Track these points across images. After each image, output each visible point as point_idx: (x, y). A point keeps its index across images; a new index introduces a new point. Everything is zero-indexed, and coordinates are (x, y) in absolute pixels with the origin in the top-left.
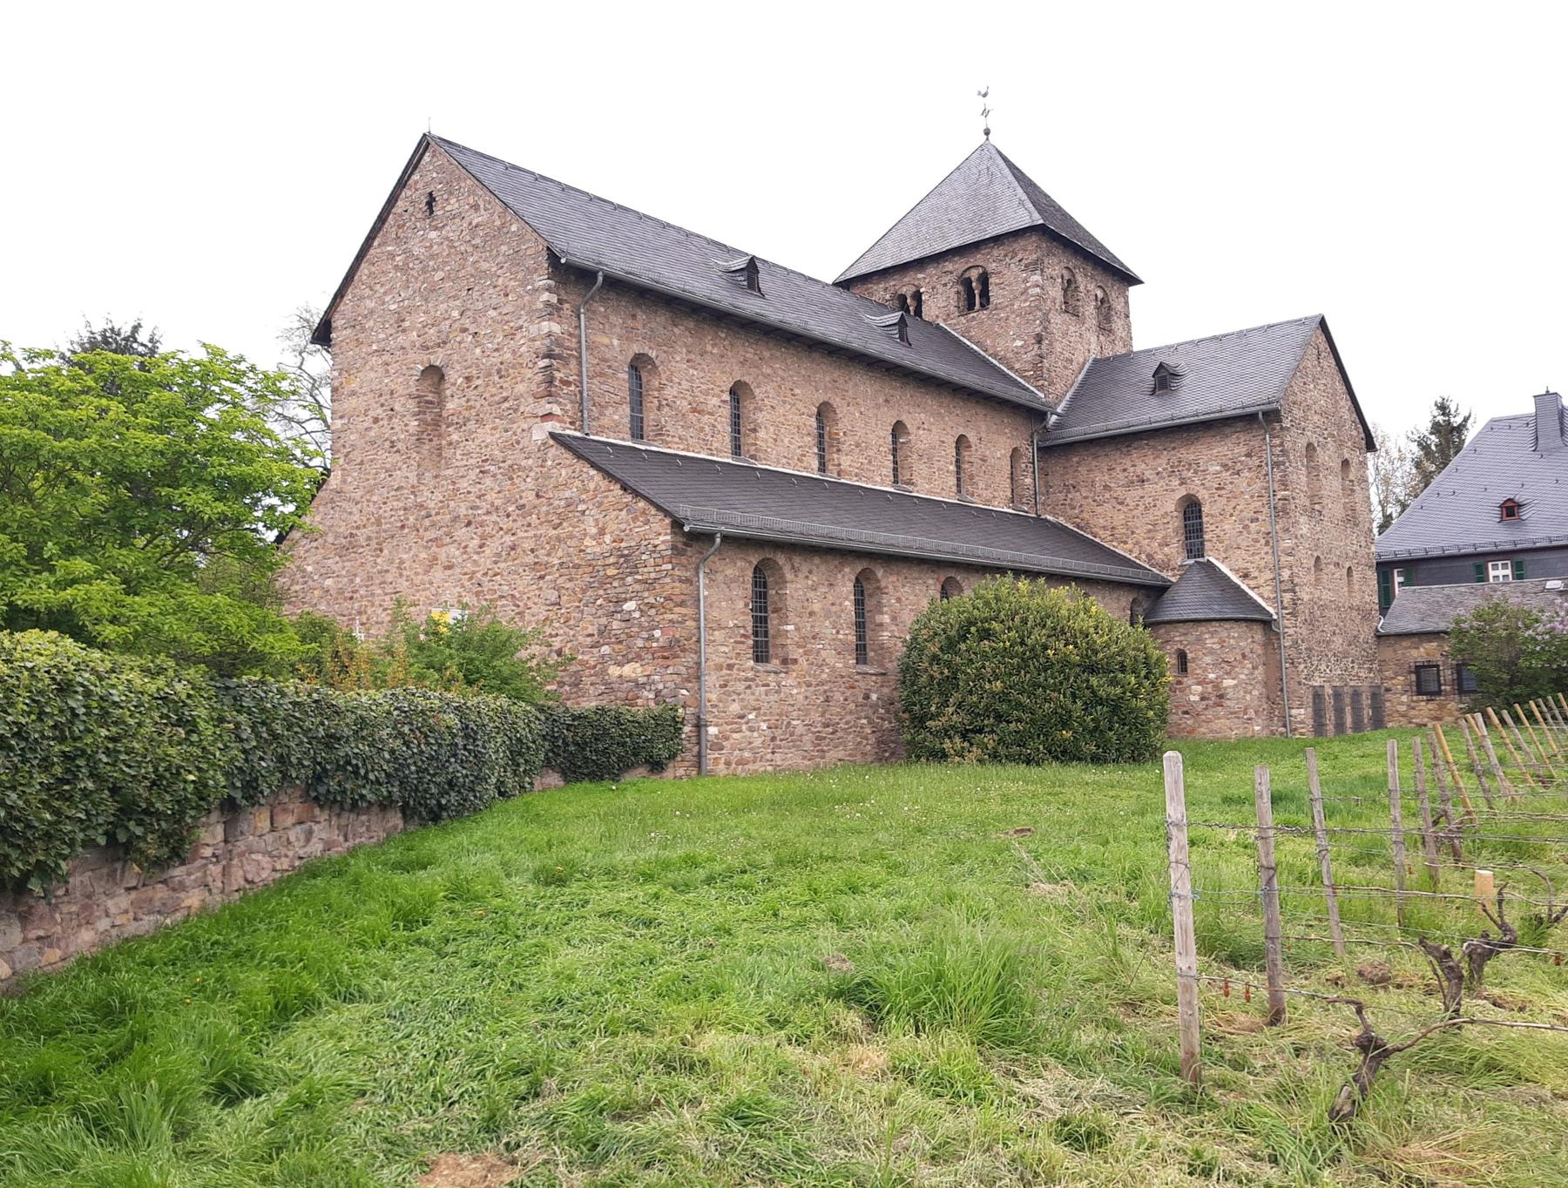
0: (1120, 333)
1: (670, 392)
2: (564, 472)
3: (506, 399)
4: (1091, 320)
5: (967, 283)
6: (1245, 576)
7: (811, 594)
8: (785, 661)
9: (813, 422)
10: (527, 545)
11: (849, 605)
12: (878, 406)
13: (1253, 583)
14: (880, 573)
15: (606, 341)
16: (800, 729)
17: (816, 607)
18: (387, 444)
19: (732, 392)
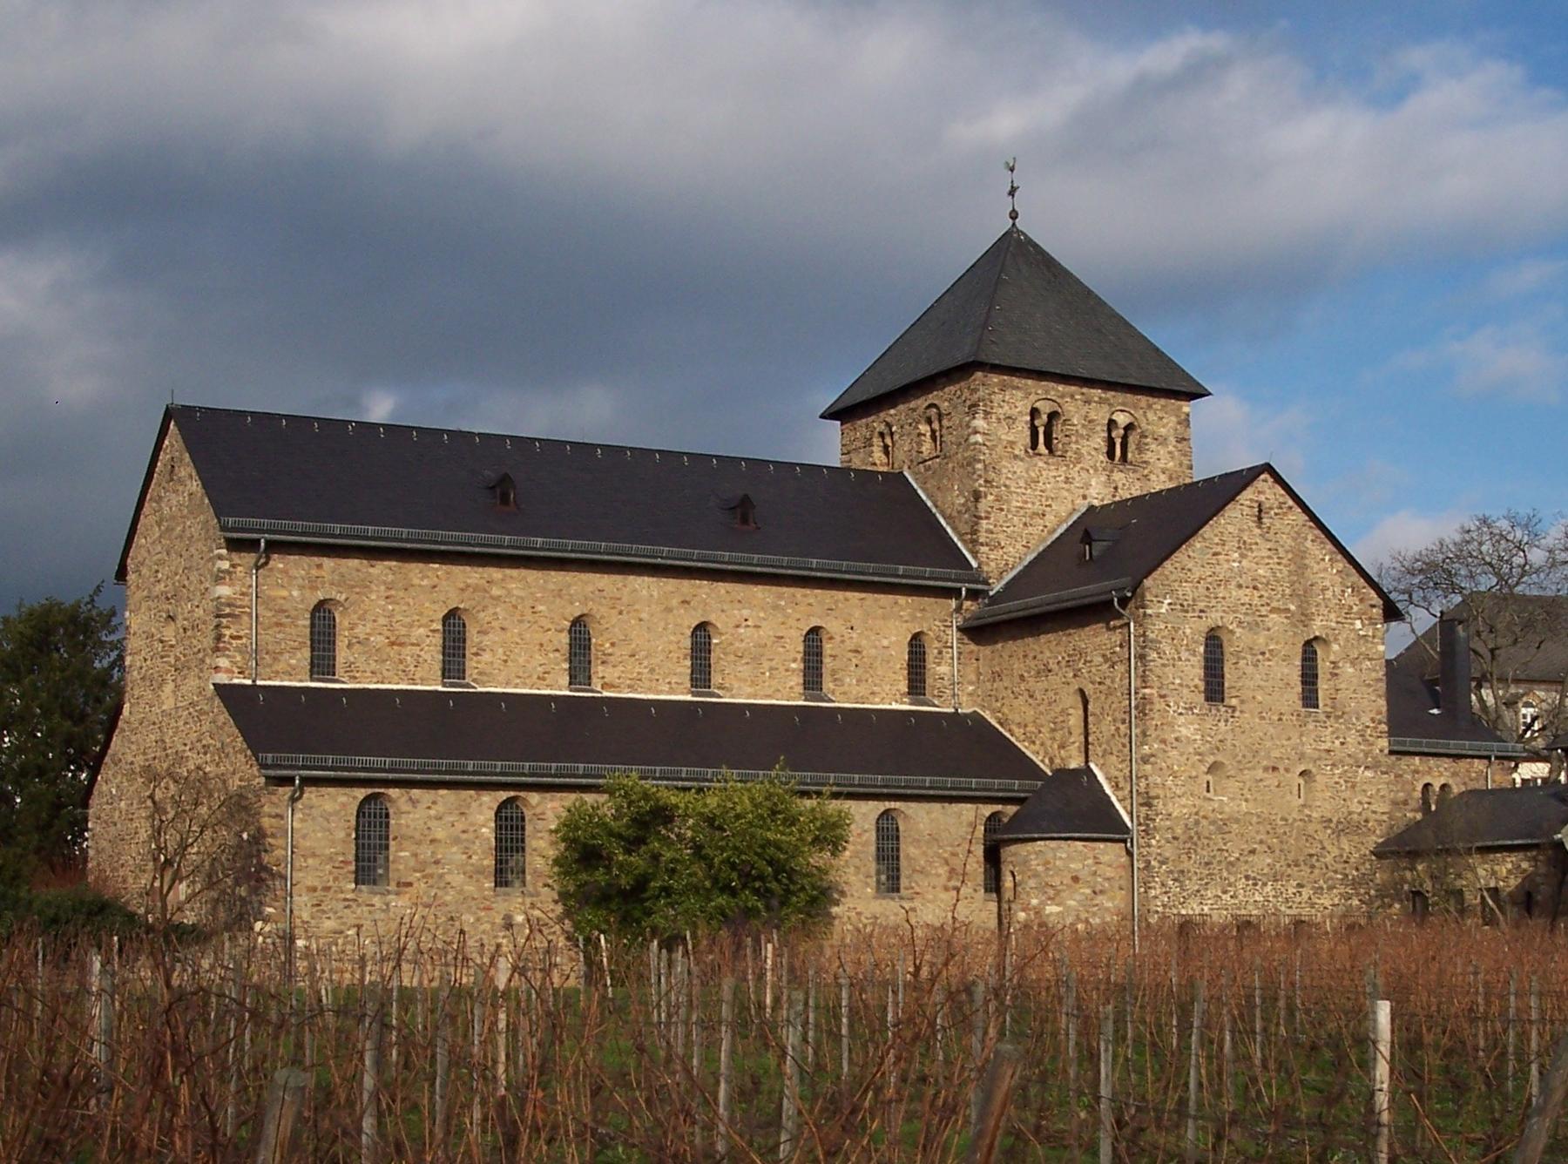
6: (1117, 787)
13: (1120, 793)
15: (284, 593)
17: (440, 834)
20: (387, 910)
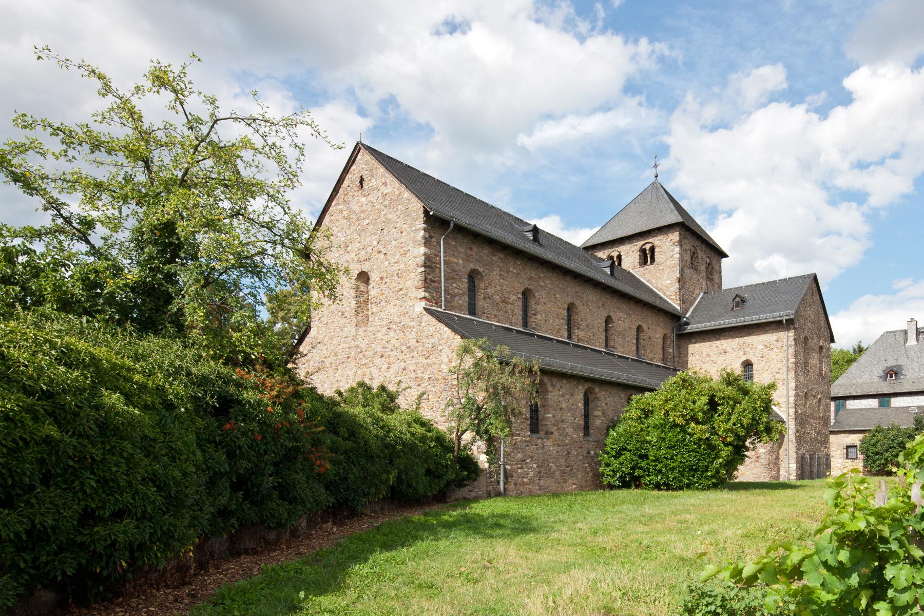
0: (717, 281)
1: (490, 291)
2: (431, 329)
3: (401, 290)
4: (704, 274)
5: (643, 251)
7: (561, 399)
8: (547, 433)
9: (565, 312)
10: (412, 368)
11: (581, 405)
12: (598, 307)
14: (597, 390)
15: (456, 260)
16: (554, 468)
17: (564, 405)
18: (340, 314)
19: (524, 294)
20: (543, 448)
